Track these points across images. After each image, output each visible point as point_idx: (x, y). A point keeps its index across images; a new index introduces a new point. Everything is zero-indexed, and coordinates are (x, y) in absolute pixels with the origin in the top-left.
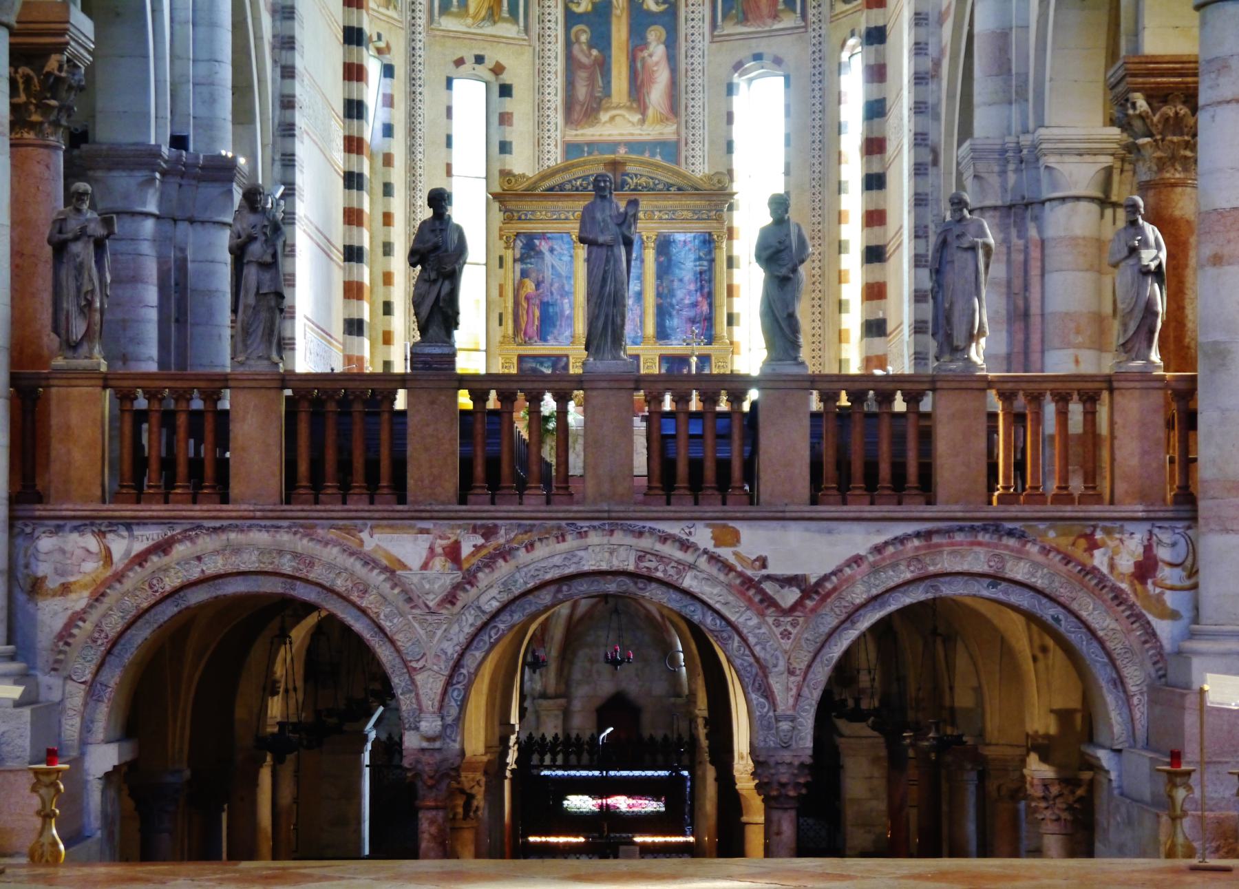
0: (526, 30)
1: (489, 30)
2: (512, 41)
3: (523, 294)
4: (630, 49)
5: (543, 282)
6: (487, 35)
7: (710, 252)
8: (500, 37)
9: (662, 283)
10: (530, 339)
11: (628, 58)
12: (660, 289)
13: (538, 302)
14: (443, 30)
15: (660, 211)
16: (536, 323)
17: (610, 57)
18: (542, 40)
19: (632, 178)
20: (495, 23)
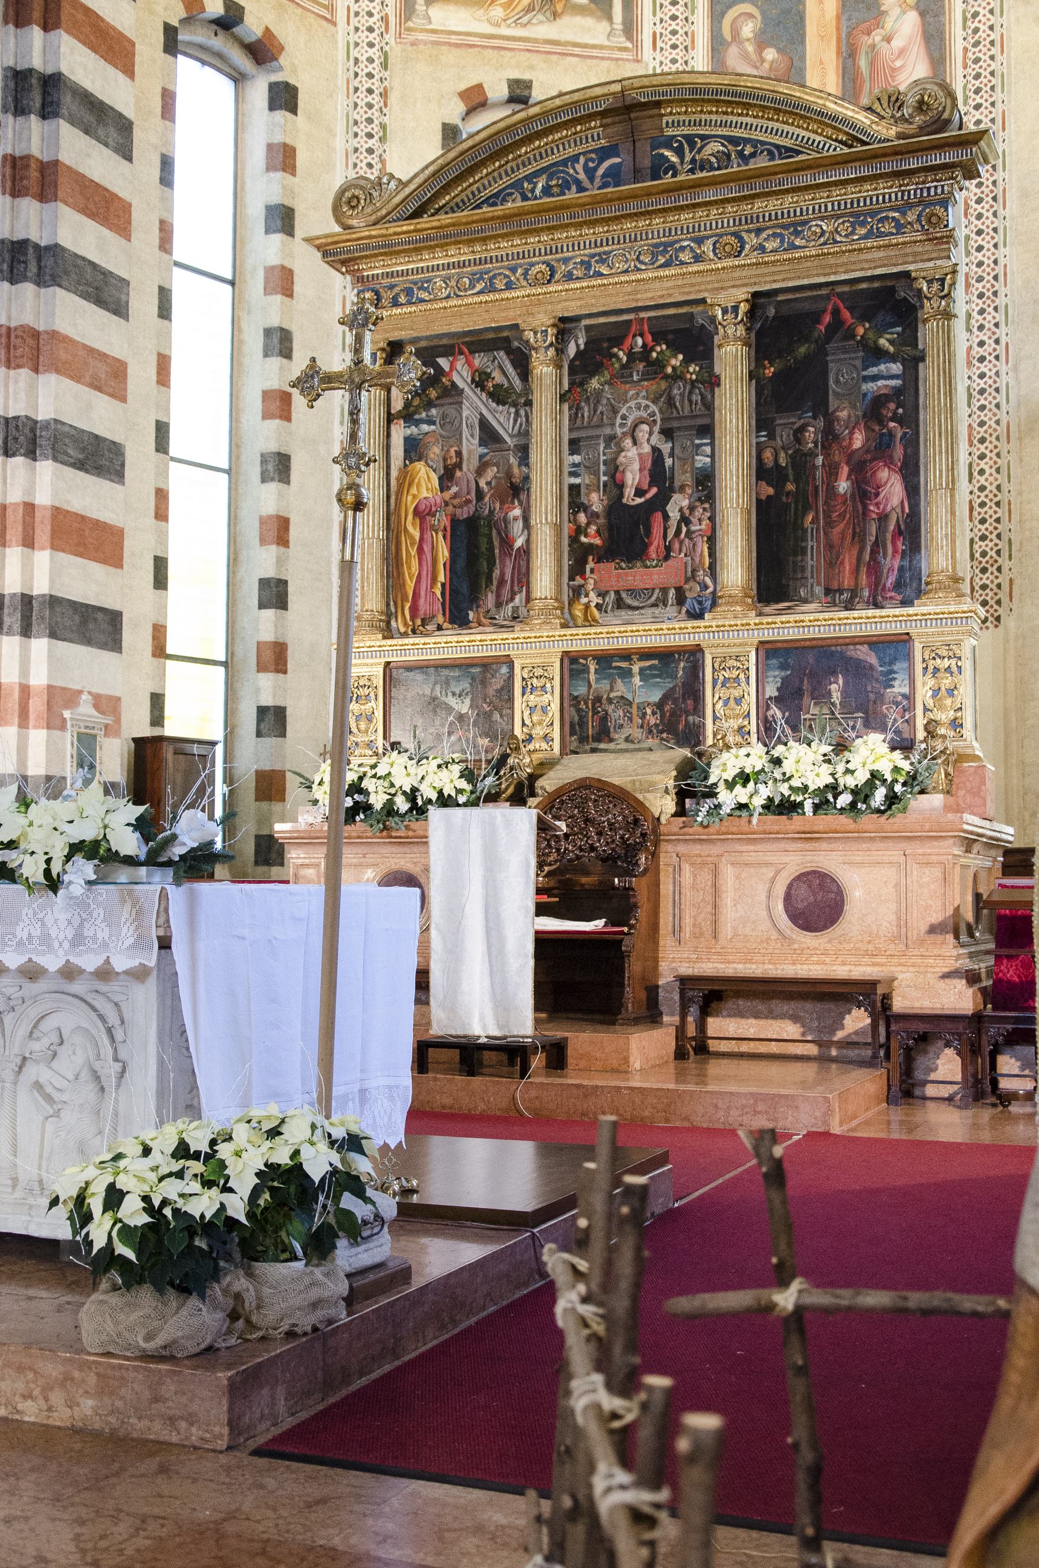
0: (630, 28)
1: (543, 29)
2: (595, 53)
3: (410, 503)
4: (844, 36)
5: (459, 465)
6: (536, 41)
7: (910, 338)
8: (567, 43)
9: (771, 436)
10: (424, 622)
11: (839, 52)
12: (768, 455)
13: (445, 522)
14: (434, 31)
15: (758, 231)
16: (441, 578)
17: (803, 58)
18: (659, 44)
19: (679, 152)
20: (555, 15)
